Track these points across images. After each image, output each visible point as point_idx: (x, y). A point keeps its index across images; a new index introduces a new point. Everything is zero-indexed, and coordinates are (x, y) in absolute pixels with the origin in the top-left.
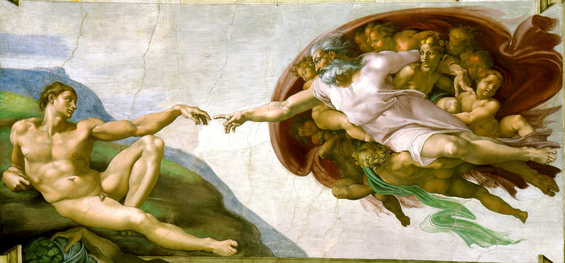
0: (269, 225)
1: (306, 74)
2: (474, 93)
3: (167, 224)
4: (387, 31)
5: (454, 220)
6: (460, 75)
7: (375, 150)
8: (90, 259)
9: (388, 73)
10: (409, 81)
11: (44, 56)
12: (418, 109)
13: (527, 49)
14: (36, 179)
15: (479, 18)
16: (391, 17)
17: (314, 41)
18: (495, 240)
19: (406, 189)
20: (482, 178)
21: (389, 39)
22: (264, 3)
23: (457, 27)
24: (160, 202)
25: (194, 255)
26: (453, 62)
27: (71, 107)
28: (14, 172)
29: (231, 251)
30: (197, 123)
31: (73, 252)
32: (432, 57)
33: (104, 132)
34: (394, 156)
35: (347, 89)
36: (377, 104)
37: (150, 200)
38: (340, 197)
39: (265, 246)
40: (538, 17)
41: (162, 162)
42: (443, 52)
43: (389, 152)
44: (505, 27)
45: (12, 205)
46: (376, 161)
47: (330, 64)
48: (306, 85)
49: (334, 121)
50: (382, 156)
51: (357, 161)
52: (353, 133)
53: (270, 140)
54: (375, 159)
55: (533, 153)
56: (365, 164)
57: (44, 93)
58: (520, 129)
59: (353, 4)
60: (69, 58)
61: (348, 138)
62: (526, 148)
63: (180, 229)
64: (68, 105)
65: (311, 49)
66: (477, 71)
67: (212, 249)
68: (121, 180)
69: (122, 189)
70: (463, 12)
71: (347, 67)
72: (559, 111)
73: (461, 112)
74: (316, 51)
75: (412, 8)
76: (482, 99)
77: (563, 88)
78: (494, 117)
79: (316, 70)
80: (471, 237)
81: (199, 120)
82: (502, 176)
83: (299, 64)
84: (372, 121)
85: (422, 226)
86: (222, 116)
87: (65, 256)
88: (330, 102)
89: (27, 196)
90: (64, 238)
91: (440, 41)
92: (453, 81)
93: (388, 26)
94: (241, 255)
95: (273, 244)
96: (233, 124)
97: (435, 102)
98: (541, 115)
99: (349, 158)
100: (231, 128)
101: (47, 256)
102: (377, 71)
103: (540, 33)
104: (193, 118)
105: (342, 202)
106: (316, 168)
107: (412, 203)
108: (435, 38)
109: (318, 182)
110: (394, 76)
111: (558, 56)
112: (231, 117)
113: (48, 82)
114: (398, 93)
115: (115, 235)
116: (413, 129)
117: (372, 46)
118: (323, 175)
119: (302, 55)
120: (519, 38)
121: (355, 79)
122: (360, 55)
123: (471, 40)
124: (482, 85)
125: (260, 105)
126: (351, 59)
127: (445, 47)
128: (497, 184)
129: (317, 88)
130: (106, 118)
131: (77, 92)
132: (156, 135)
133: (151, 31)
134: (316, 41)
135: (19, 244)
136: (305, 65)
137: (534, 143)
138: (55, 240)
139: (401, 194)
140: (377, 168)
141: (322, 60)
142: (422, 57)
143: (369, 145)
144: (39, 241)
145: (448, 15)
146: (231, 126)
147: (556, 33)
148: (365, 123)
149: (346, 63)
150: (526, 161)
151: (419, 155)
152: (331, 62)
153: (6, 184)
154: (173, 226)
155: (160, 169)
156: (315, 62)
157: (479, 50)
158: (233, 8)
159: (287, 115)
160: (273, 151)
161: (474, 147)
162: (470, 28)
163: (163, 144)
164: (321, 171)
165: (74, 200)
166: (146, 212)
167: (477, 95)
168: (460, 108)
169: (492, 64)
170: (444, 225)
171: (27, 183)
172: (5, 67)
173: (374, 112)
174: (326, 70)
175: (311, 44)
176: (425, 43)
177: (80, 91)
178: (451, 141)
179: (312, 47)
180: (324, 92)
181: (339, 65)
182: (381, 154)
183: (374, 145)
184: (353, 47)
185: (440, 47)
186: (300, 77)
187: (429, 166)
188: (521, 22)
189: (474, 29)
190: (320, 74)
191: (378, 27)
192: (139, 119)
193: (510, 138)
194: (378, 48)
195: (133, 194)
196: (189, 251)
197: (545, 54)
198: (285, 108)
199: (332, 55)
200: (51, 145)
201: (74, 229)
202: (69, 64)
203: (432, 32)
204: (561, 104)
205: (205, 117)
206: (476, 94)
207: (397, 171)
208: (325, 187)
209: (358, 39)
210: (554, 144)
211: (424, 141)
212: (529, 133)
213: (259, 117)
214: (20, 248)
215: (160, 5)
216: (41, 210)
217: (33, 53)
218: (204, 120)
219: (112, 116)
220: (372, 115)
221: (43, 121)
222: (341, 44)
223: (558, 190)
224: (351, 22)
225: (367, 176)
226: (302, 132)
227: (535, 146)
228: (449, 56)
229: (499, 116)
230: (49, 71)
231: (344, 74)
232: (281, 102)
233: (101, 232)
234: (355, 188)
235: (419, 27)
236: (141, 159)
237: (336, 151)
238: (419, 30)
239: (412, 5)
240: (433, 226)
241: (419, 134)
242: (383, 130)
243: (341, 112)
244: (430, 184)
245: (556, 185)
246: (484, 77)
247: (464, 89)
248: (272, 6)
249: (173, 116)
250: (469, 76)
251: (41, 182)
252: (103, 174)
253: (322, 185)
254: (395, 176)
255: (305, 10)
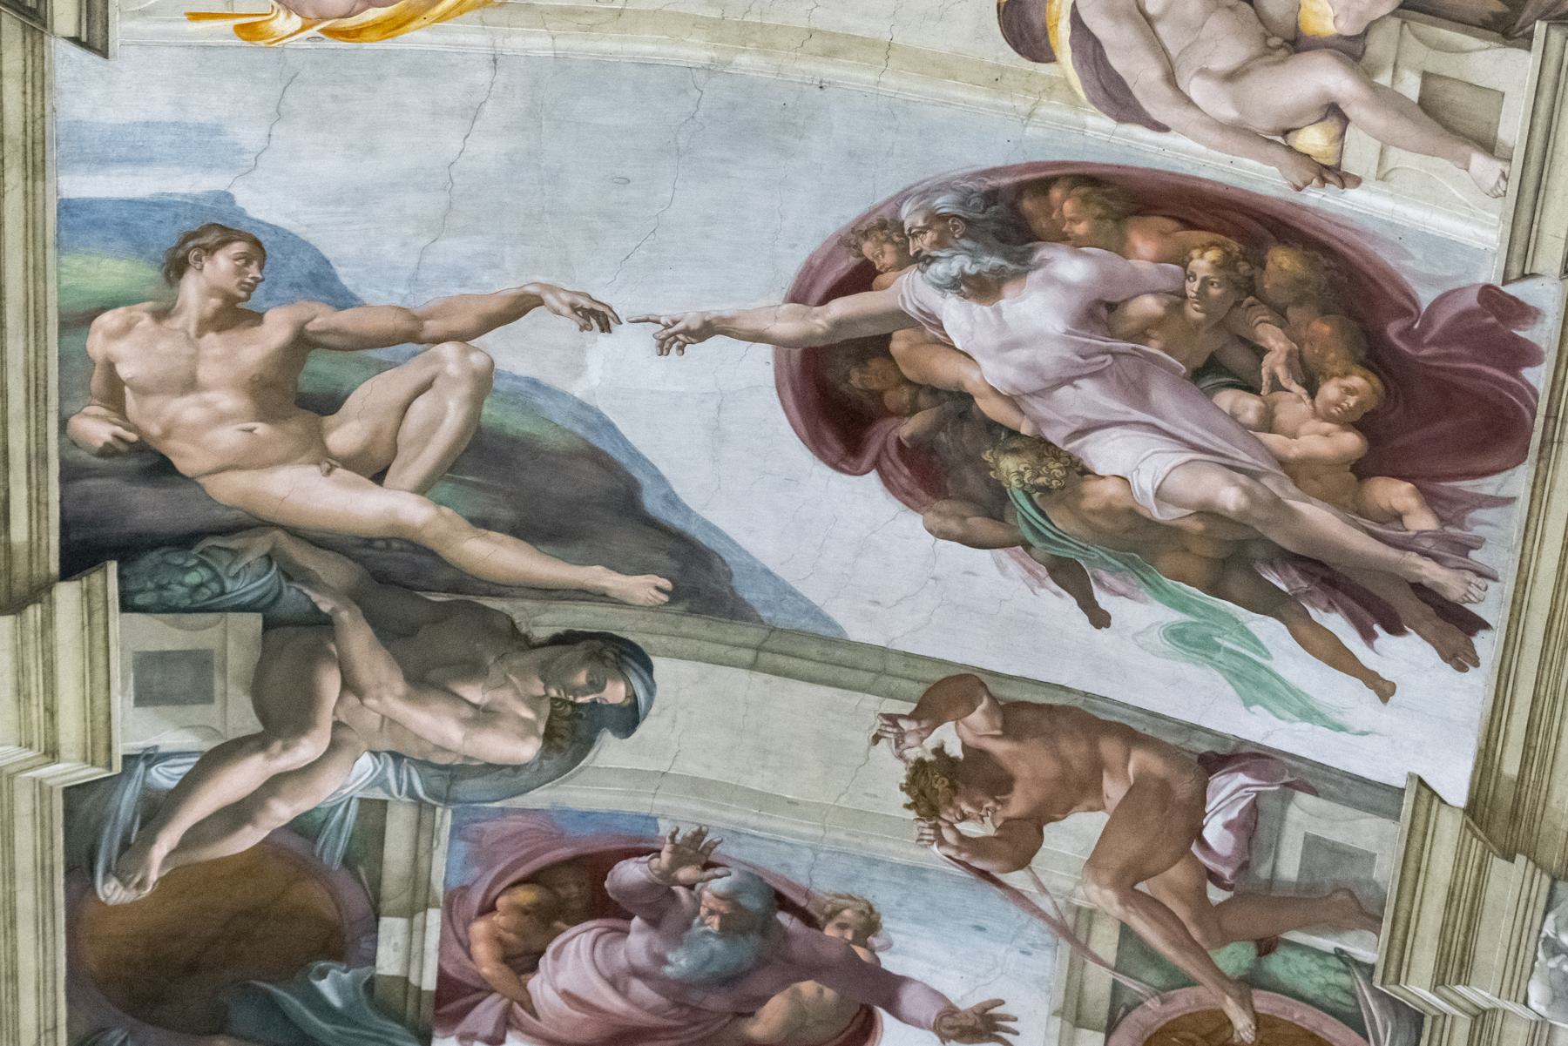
0: (755, 560)
1: (883, 253)
2: (1308, 401)
3: (493, 534)
4: (1106, 206)
5: (1218, 647)
6: (1281, 351)
7: (1041, 457)
8: (293, 592)
9: (1097, 297)
10: (1148, 328)
11: (178, 169)
12: (1162, 394)
13: (1453, 350)
14: (155, 429)
15: (1347, 245)
16: (1121, 177)
17: (912, 187)
18: (1310, 714)
19: (1109, 554)
20: (1298, 583)
21: (1110, 225)
22: (783, 76)
23: (1290, 246)
24: (477, 485)
25: (560, 598)
26: (1267, 318)
27: (250, 275)
28: (97, 416)
29: (656, 597)
30: (582, 328)
31: (248, 577)
32: (1214, 291)
33: (336, 331)
34: (1089, 480)
35: (985, 308)
36: (1062, 359)
37: (450, 480)
38: (941, 536)
39: (741, 599)
40: (1495, 292)
41: (486, 402)
42: (1245, 289)
43: (1079, 469)
44: (1408, 285)
45: (91, 483)
46: (1041, 480)
47: (951, 247)
48: (880, 279)
49: (946, 369)
50: (1059, 473)
51: (993, 469)
52: (991, 408)
53: (773, 384)
54: (1039, 476)
55: (1430, 572)
56: (1014, 480)
57: (178, 248)
58: (1407, 513)
59: (1025, 126)
60: (246, 170)
61: (977, 418)
62: (1414, 554)
63: (524, 544)
64: (240, 272)
65: (902, 203)
66: (1323, 356)
67: (606, 588)
68: (377, 433)
69: (380, 454)
70: (1309, 217)
71: (992, 262)
72: (1509, 506)
73: (1270, 430)
74: (916, 210)
75: (1179, 171)
76: (1325, 420)
77: (1527, 462)
78: (1349, 468)
79: (912, 253)
80: (1255, 692)
81: (589, 320)
82: (1345, 592)
83: (866, 232)
84: (1042, 393)
85: (1140, 638)
86: (651, 318)
87: (229, 585)
88: (940, 327)
89: (133, 463)
90: (226, 549)
91: (1241, 263)
92: (1262, 360)
93: (1111, 197)
94: (680, 607)
95: (762, 598)
96: (681, 337)
97: (1209, 394)
98: (1465, 503)
99: (973, 460)
100: (675, 345)
101: (182, 584)
102: (1068, 287)
103: (1494, 327)
104: (574, 316)
105: (947, 547)
106: (889, 463)
107: (1121, 587)
108: (1228, 254)
109: (890, 495)
110: (1112, 307)
111: (1527, 391)
112: (675, 323)
113: (189, 225)
114: (1116, 347)
115: (358, 546)
116: (1144, 434)
117: (1064, 229)
118: (903, 481)
119: (878, 213)
120: (1441, 320)
121: (1009, 290)
122: (1029, 240)
123: (1320, 285)
124: (1330, 391)
125: (754, 305)
126: (1005, 246)
127: (1251, 278)
128: (1334, 607)
129: (909, 295)
130: (343, 299)
131: (266, 246)
132: (475, 343)
133: (474, 113)
134: (916, 188)
135: (111, 559)
136: (882, 238)
137: (1436, 552)
138: (202, 553)
139: (1095, 560)
140: (1041, 496)
141: (929, 234)
142: (1188, 285)
143: (1027, 443)
144: (165, 554)
145: (1269, 213)
146: (674, 342)
147: (1534, 340)
148: (1024, 394)
149: (991, 254)
150: (1411, 581)
151: (1151, 494)
152: (951, 242)
153: (76, 441)
154: (509, 539)
155: (480, 416)
156: (910, 234)
157: (1334, 313)
158: (700, 77)
159: (823, 337)
160: (780, 408)
161: (1292, 514)
162: (1321, 258)
163: (492, 363)
164: (902, 473)
165: (255, 472)
166: (439, 503)
167: (1314, 407)
168: (1268, 422)
169: (1362, 354)
170: (1193, 649)
171: (132, 437)
172: (72, 196)
173: (1050, 375)
174: (938, 257)
175: (902, 192)
176: (1201, 257)
177: (274, 243)
178: (1236, 484)
179: (906, 198)
180: (926, 302)
181: (972, 254)
182: (1056, 468)
183: (1041, 447)
184: (1013, 220)
185: (1240, 277)
186: (867, 259)
187: (1174, 523)
188: (1450, 287)
189: (1332, 263)
190: (921, 264)
191: (1083, 190)
192: (431, 304)
193: (1381, 523)
194: (1078, 237)
195: (405, 465)
196: (546, 589)
197: (1497, 377)
198: (819, 321)
199: (955, 227)
200: (195, 358)
201: (252, 532)
202: (247, 182)
203: (1222, 237)
204: (1515, 495)
205: (604, 314)
206: (1313, 404)
207: (1093, 512)
208: (905, 507)
209: (1028, 205)
210: (1483, 570)
211: (1168, 468)
212: (1427, 528)
213: (748, 331)
214: (113, 567)
215: (497, 57)
216: (167, 491)
217: (150, 161)
218: (603, 322)
219: (359, 295)
220: (1045, 380)
221: (174, 305)
222: (982, 208)
223: (1476, 664)
224: (1014, 166)
225: (1013, 506)
226: (858, 380)
227: (1437, 559)
228: (1257, 301)
229: (1363, 469)
230: (190, 201)
231: (984, 275)
232: (809, 308)
233: (322, 539)
234: (981, 526)
235: (1191, 219)
236: (428, 392)
237: (942, 437)
238: (1189, 225)
239: (1180, 165)
240: (1167, 646)
241: (1157, 449)
242: (1069, 418)
243: (967, 355)
244: (1170, 560)
245: (1474, 652)
246: (1337, 375)
247: (1284, 384)
248: (805, 87)
249: (520, 306)
250: (1301, 360)
251: (167, 434)
252: (330, 420)
253: (897, 502)
254: (1085, 522)
255: (896, 112)
